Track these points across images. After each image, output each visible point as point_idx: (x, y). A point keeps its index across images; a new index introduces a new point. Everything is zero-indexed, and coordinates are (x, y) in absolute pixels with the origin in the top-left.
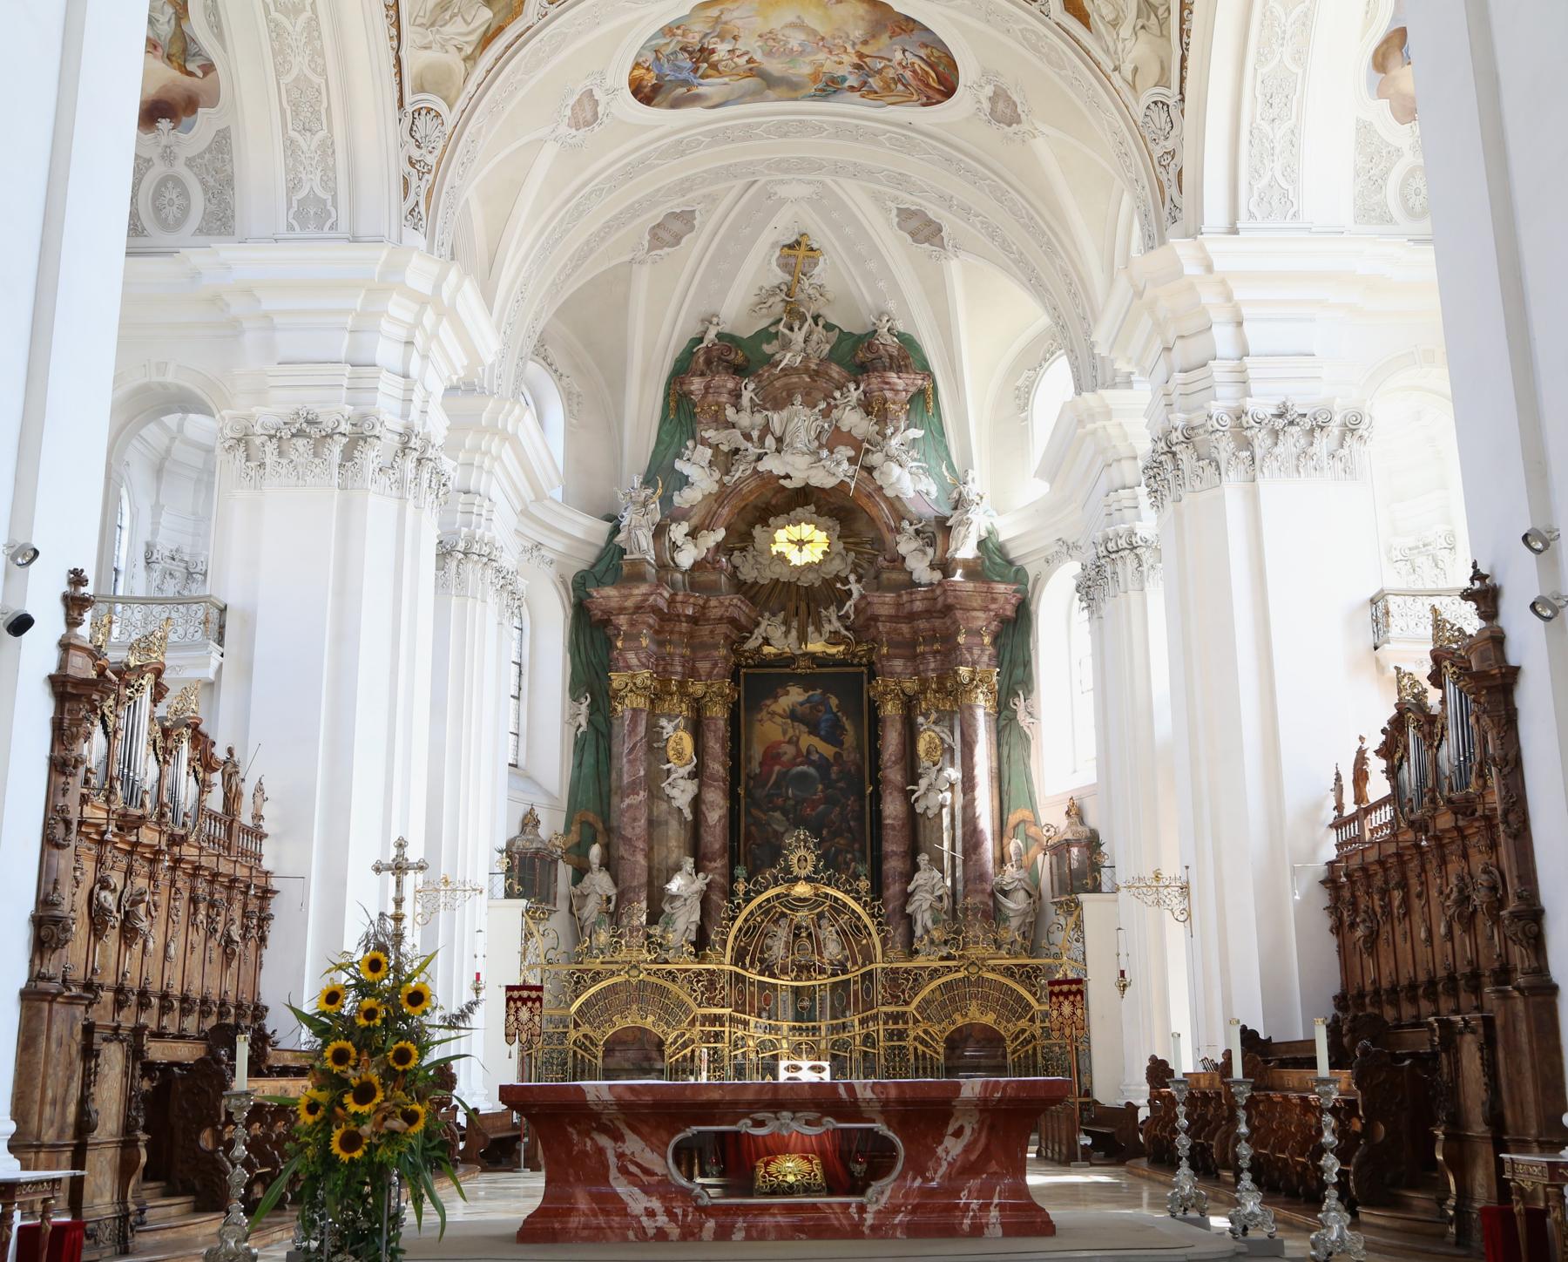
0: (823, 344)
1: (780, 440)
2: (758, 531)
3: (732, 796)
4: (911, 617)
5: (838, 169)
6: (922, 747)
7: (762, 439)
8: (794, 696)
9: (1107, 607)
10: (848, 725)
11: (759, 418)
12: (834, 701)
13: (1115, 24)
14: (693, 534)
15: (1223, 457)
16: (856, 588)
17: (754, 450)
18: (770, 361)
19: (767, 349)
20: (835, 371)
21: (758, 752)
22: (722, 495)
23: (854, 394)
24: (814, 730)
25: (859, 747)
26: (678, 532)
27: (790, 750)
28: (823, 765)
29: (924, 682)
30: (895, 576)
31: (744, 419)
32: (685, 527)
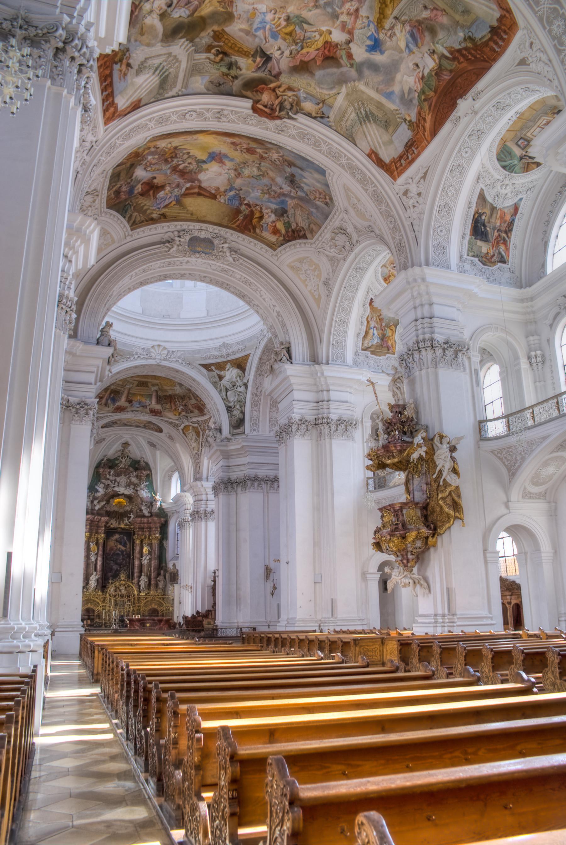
0: (129, 462)
1: (118, 483)
2: (111, 500)
3: (103, 558)
4: (143, 523)
5: (136, 435)
6: (144, 550)
7: (115, 483)
8: (117, 536)
9: (183, 531)
10: (128, 543)
11: (114, 478)
12: (125, 538)
13: (191, 440)
14: (99, 502)
15: (202, 517)
16: (132, 516)
17: (113, 485)
18: (117, 465)
19: (117, 462)
20: (131, 469)
21: (108, 548)
22: (105, 494)
23: (135, 474)
24: (121, 543)
25: (130, 548)
26: (96, 502)
27: (115, 548)
28: (122, 552)
29: (146, 537)
30: (141, 513)
31: (111, 478)
32: (97, 501)
